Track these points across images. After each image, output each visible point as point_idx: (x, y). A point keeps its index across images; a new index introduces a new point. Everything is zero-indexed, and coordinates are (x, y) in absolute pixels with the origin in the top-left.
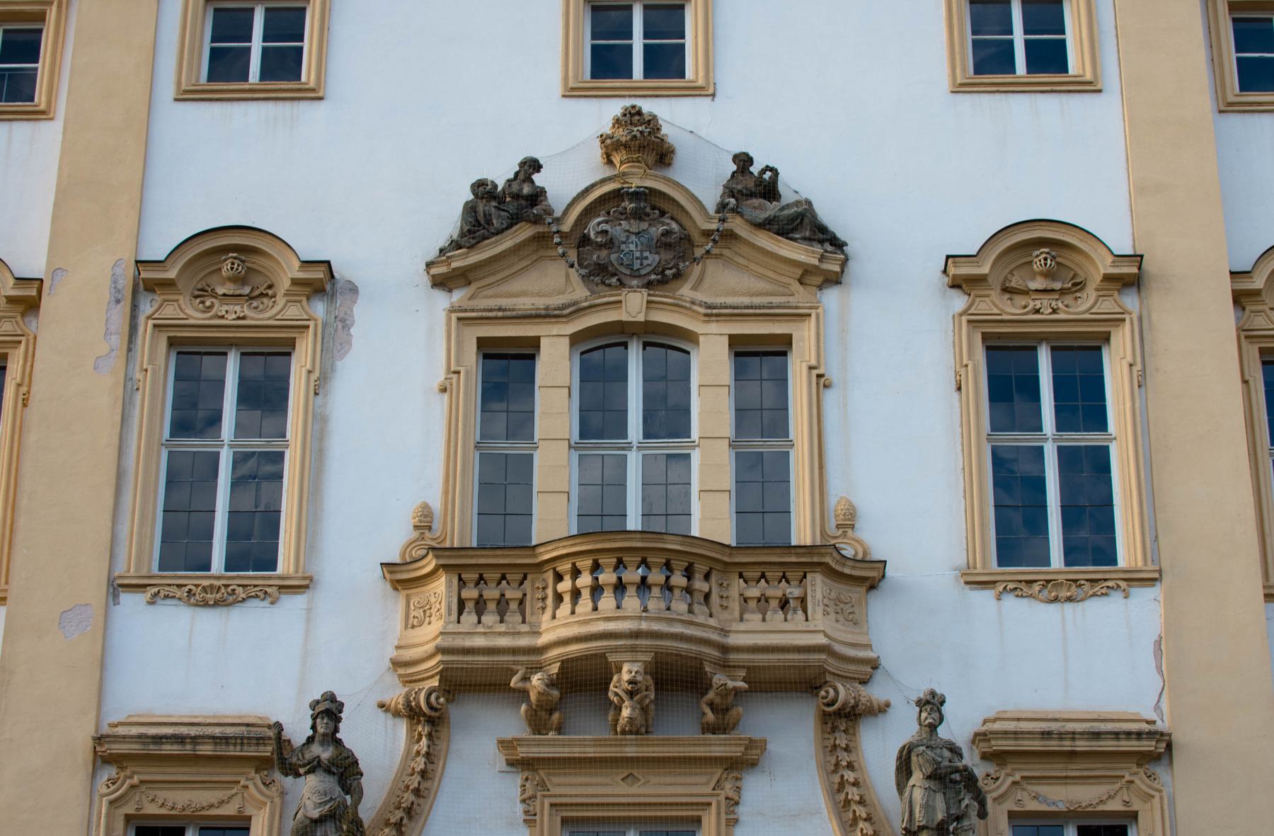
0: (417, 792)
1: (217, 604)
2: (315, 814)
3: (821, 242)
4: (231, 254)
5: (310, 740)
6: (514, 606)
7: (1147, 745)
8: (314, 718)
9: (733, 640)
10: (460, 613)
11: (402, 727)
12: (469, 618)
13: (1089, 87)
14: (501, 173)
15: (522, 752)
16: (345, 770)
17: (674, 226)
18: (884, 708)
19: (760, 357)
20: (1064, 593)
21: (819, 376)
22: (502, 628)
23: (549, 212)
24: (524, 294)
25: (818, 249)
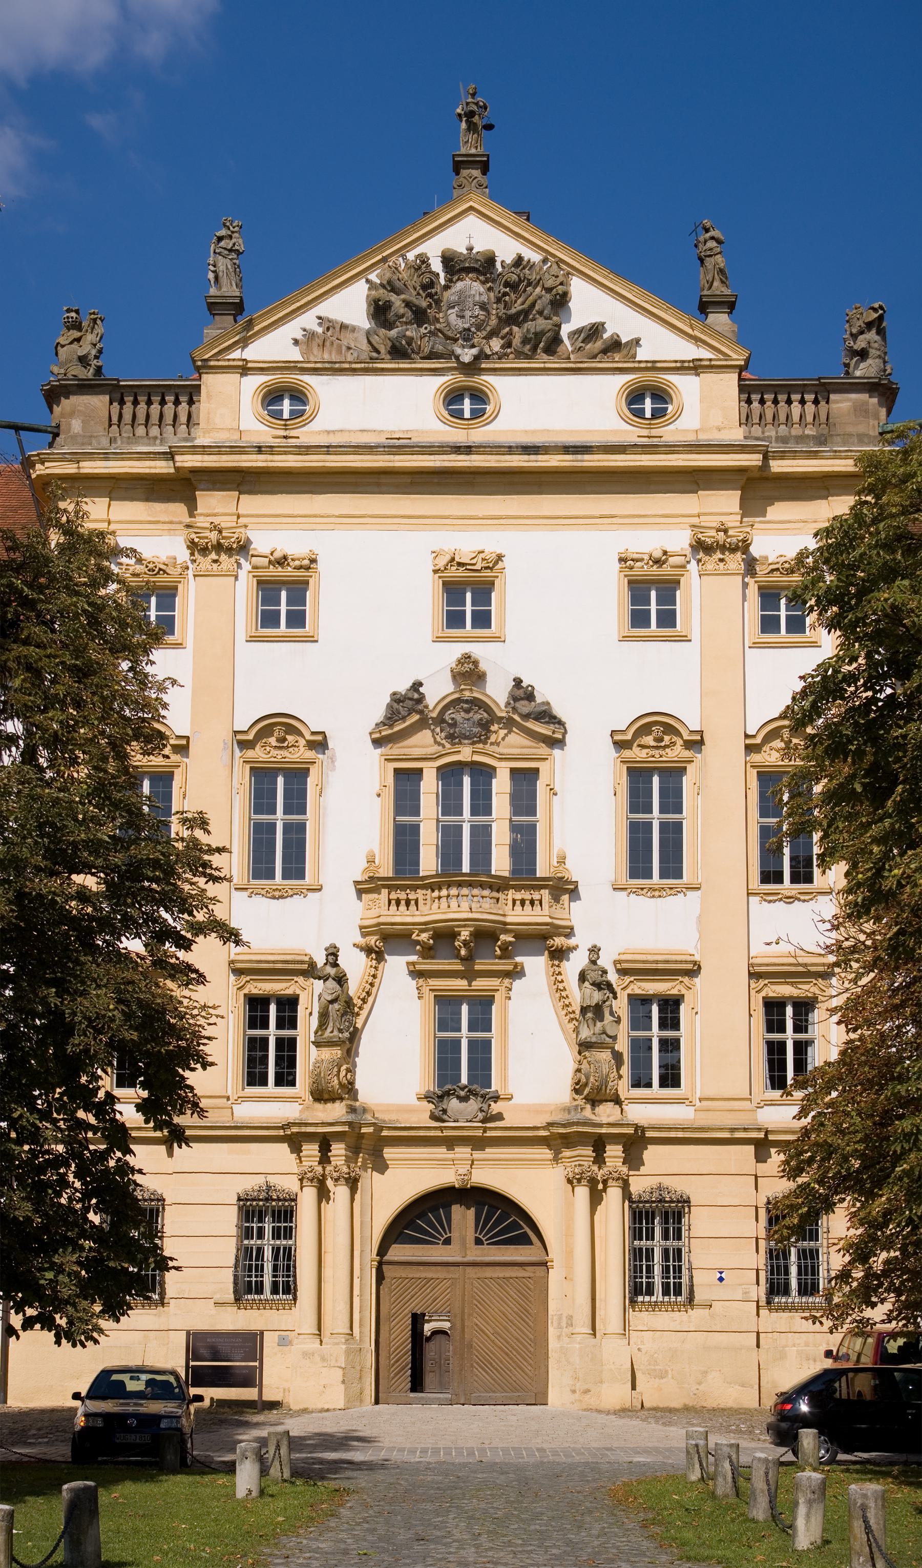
0: (372, 985)
1: (282, 897)
2: (329, 998)
3: (554, 723)
4: (278, 726)
5: (326, 964)
6: (413, 902)
7: (690, 966)
8: (327, 956)
9: (509, 919)
10: (389, 906)
11: (363, 955)
12: (393, 907)
13: (685, 639)
14: (403, 687)
15: (418, 967)
16: (341, 980)
17: (485, 715)
18: (575, 948)
19: (525, 780)
20: (657, 893)
21: (551, 789)
22: (408, 913)
23: (427, 707)
24: (415, 746)
25: (552, 727)
